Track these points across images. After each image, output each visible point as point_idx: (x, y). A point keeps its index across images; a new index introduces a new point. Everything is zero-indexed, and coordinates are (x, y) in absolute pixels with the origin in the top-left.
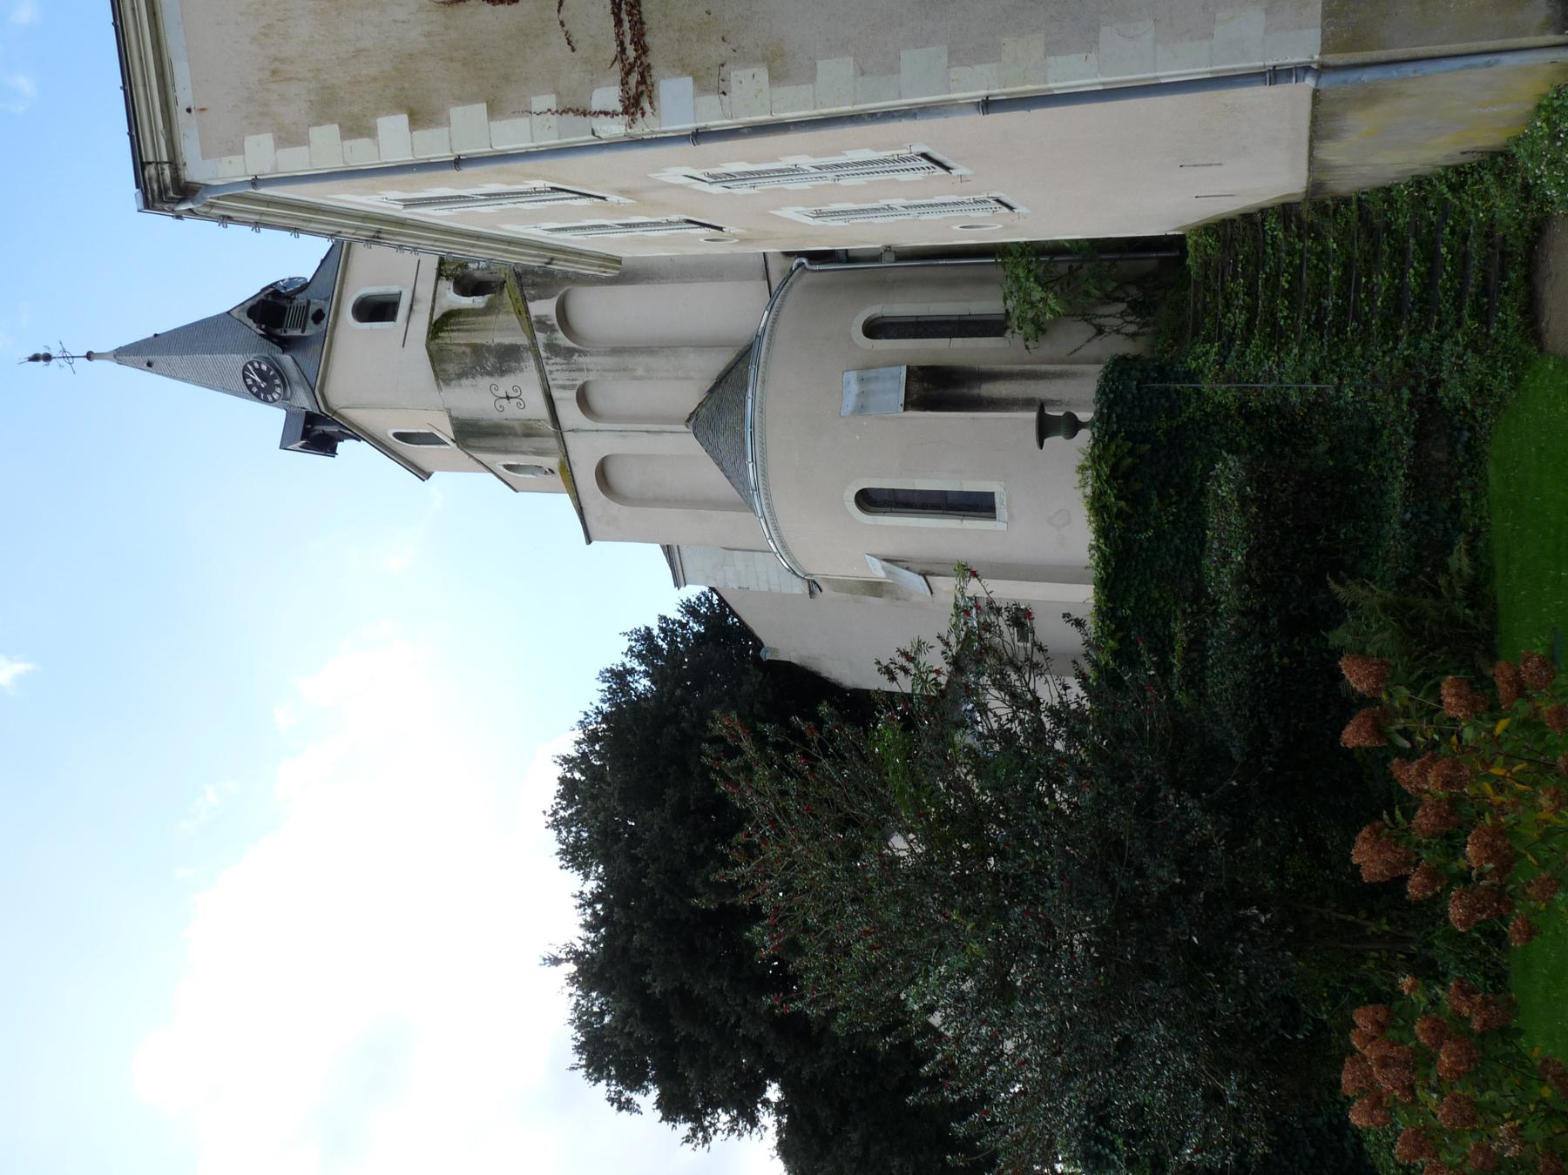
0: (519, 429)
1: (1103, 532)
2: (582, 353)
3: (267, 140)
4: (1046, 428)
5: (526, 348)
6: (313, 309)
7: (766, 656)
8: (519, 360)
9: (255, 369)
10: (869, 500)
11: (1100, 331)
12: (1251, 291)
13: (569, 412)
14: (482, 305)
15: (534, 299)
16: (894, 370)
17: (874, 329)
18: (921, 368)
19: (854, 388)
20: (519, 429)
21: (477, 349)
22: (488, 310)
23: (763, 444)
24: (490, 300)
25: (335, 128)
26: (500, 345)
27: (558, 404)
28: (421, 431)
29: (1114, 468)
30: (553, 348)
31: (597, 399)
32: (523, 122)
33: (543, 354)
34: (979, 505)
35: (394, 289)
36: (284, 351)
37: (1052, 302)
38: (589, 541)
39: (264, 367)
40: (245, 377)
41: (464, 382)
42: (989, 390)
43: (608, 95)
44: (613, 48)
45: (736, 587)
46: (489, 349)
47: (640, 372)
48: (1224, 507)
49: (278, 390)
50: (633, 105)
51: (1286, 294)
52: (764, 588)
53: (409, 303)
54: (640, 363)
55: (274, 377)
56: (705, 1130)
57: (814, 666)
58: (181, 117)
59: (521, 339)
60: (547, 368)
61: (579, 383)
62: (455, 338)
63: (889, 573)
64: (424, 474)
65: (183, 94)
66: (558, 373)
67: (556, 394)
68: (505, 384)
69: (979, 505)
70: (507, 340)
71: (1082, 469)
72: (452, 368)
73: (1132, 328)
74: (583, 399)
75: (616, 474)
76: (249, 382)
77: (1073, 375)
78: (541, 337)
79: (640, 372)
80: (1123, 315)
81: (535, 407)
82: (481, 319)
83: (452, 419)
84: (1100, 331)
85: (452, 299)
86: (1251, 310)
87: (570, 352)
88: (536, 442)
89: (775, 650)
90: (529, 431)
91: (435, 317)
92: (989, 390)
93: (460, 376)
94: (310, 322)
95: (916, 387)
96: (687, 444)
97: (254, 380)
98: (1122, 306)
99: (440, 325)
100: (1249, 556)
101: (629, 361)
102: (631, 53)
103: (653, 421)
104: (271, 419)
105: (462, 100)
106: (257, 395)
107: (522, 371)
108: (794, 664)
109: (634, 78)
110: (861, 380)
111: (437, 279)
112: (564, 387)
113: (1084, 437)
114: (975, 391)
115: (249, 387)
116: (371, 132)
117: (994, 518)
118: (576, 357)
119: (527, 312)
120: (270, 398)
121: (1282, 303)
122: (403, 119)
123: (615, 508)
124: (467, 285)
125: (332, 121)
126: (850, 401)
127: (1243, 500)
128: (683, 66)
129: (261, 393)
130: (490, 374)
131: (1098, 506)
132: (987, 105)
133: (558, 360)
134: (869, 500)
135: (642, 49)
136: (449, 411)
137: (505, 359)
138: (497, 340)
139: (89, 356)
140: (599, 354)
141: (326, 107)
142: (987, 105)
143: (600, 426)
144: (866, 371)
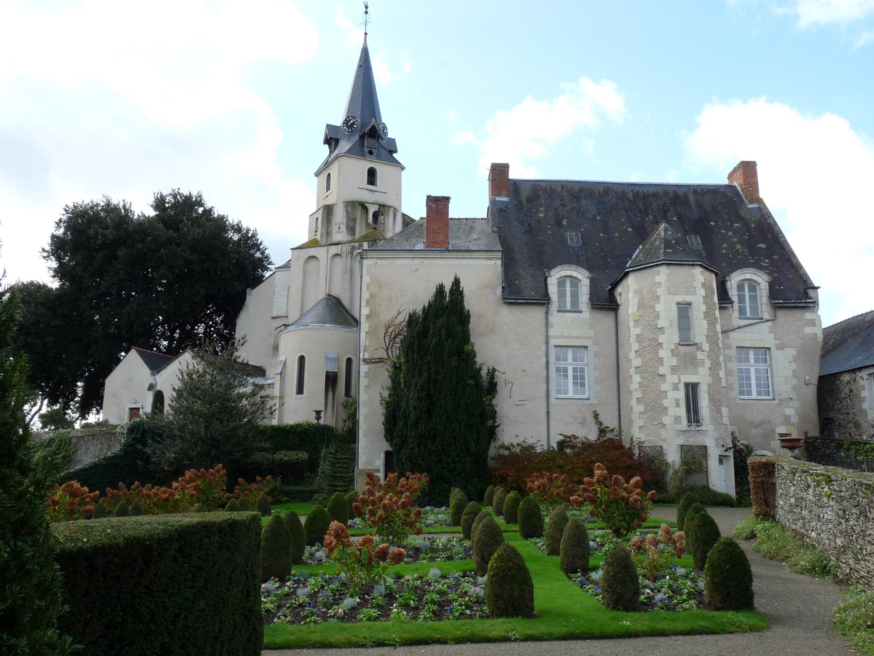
0: (329, 230)
1: (292, 427)
2: (351, 258)
3: (368, 282)
4: (318, 413)
5: (354, 238)
6: (373, 150)
7: (248, 290)
8: (351, 234)
9: (354, 122)
10: (302, 359)
11: (345, 421)
12: (345, 459)
13: (334, 250)
14: (369, 221)
15: (368, 244)
16: (337, 368)
18: (337, 376)
19: (333, 356)
20: (329, 230)
21: (355, 220)
22: (367, 224)
23: (319, 329)
24: (370, 224)
26: (356, 228)
27: (336, 246)
29: (307, 429)
30: (353, 248)
31: (337, 260)
32: (364, 339)
33: (352, 244)
34: (300, 390)
35: (378, 183)
36: (360, 136)
37: (351, 411)
38: (292, 249)
39: (355, 126)
40: (352, 117)
41: (345, 212)
42: (330, 393)
43: (367, 356)
44: (374, 357)
45: (275, 290)
46: (355, 224)
47: (345, 277)
48: (297, 455)
49: (347, 130)
50: (364, 360)
51: (342, 466)
52: (275, 301)
53: (373, 189)
54: (347, 277)
55: (352, 129)
56: (48, 257)
57: (244, 309)
58: (375, 260)
59: (357, 236)
60: (347, 245)
61: (342, 255)
62: (359, 212)
63: (281, 362)
64: (317, 174)
65: (380, 262)
66: (346, 248)
67: (339, 246)
68: (343, 228)
69: (300, 390)
70: (357, 231)
71: (307, 421)
72: (350, 209)
73: (345, 429)
74: (337, 255)
75: (313, 262)
76: (351, 118)
77: (333, 418)
78: (357, 244)
79: (345, 277)
80: (349, 427)
81: (337, 237)
82: (364, 221)
83: (333, 205)
84: (345, 421)
85: (372, 209)
86: (341, 459)
87: (352, 254)
88: (325, 235)
89: (250, 294)
90: (328, 233)
91: (366, 204)
92: (330, 393)
93: (347, 211)
94: (369, 149)
95: (332, 374)
96: (322, 294)
97: (351, 120)
98: (351, 426)
99: (363, 206)
100: (286, 461)
101: (348, 272)
102: (373, 361)
103: (330, 280)
104: (338, 120)
105: (370, 326)
106: (346, 120)
107: (348, 235)
108: (245, 301)
109: (369, 361)
110: (335, 358)
111: (379, 205)
112: (341, 250)
113: (315, 422)
114: (330, 390)
115: (349, 117)
116: (367, 306)
117: (297, 394)
118: (350, 256)
119: (365, 241)
121: (340, 465)
122: (368, 313)
123: (303, 260)
124: (376, 215)
125: (370, 297)
126: (329, 355)
127: (298, 459)
128: (369, 370)
129: (346, 122)
130: (347, 223)
131: (298, 425)
133: (350, 249)
134: (302, 359)
135: (373, 363)
136: (336, 204)
137: (351, 230)
138: (357, 228)
140: (351, 264)
141: (373, 296)
143: (329, 260)
144: (337, 360)
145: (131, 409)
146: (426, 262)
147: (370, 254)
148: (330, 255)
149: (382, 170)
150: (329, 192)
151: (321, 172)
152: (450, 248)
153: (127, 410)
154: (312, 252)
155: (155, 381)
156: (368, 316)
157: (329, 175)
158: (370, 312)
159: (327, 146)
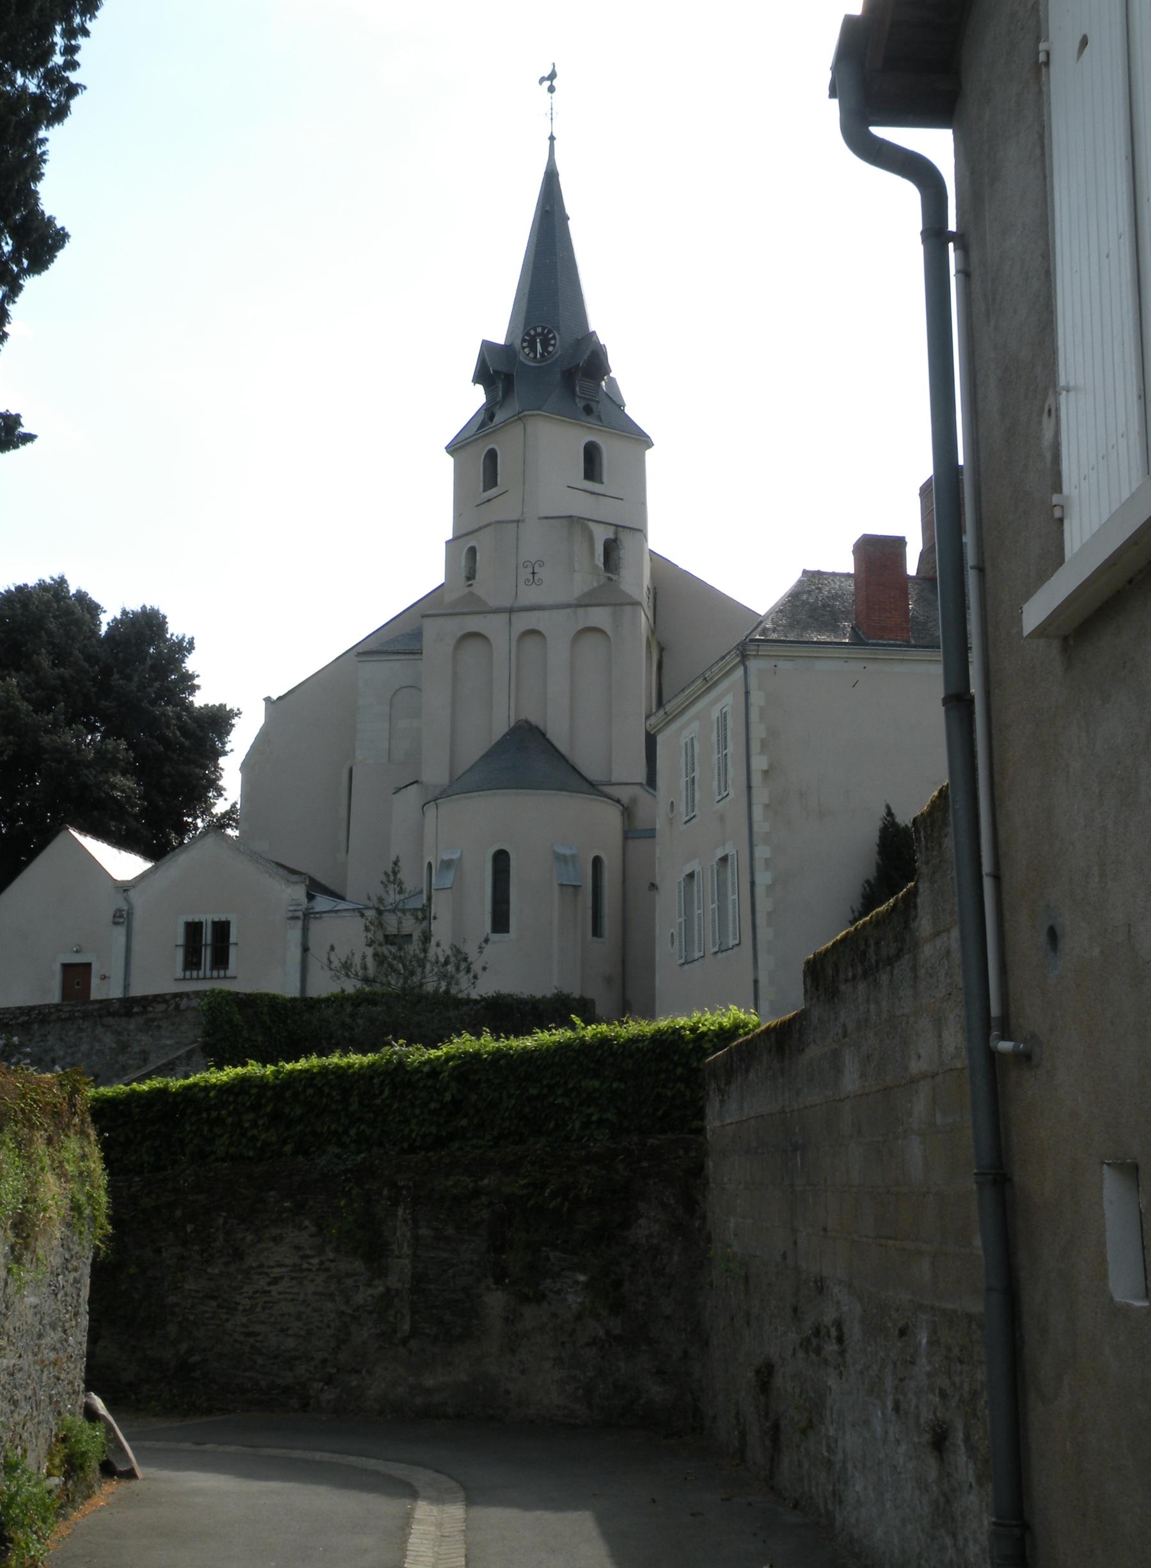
10: (501, 860)
14: (597, 562)
17: (597, 862)
25: (764, 736)
28: (499, 477)
34: (500, 923)
35: (605, 478)
65: (784, 665)
69: (500, 923)
85: (601, 535)
116: (762, 752)
120: (525, 344)
122: (766, 768)
132: (756, 982)
134: (501, 860)
139: (552, 138)
142: (756, 982)
143: (514, 644)
145: (66, 967)
146: (871, 667)
147: (765, 649)
148: (515, 635)
149: (611, 450)
150: (493, 492)
151: (468, 444)
152: (913, 642)
153: (57, 968)
154: (474, 624)
155: (127, 900)
156: (766, 773)
157: (492, 456)
158: (771, 766)
159: (480, 388)
